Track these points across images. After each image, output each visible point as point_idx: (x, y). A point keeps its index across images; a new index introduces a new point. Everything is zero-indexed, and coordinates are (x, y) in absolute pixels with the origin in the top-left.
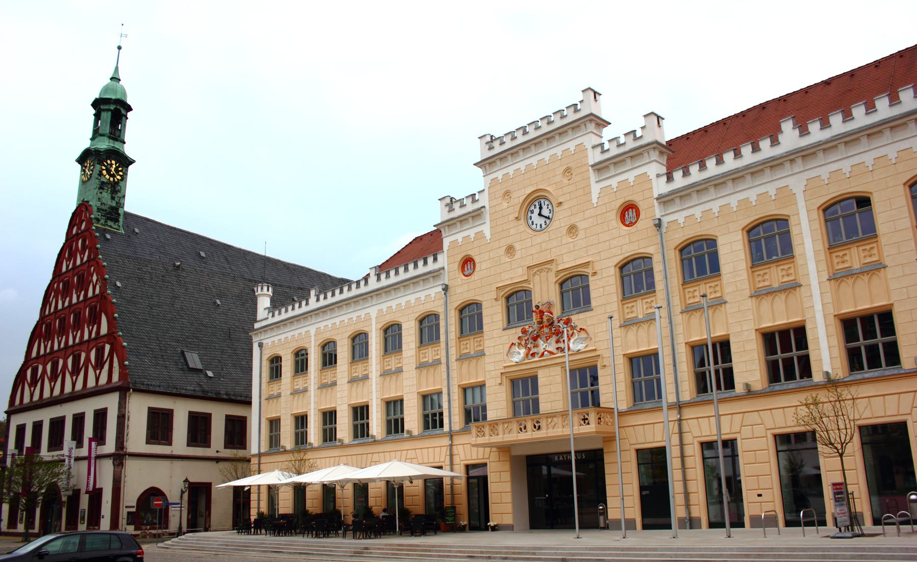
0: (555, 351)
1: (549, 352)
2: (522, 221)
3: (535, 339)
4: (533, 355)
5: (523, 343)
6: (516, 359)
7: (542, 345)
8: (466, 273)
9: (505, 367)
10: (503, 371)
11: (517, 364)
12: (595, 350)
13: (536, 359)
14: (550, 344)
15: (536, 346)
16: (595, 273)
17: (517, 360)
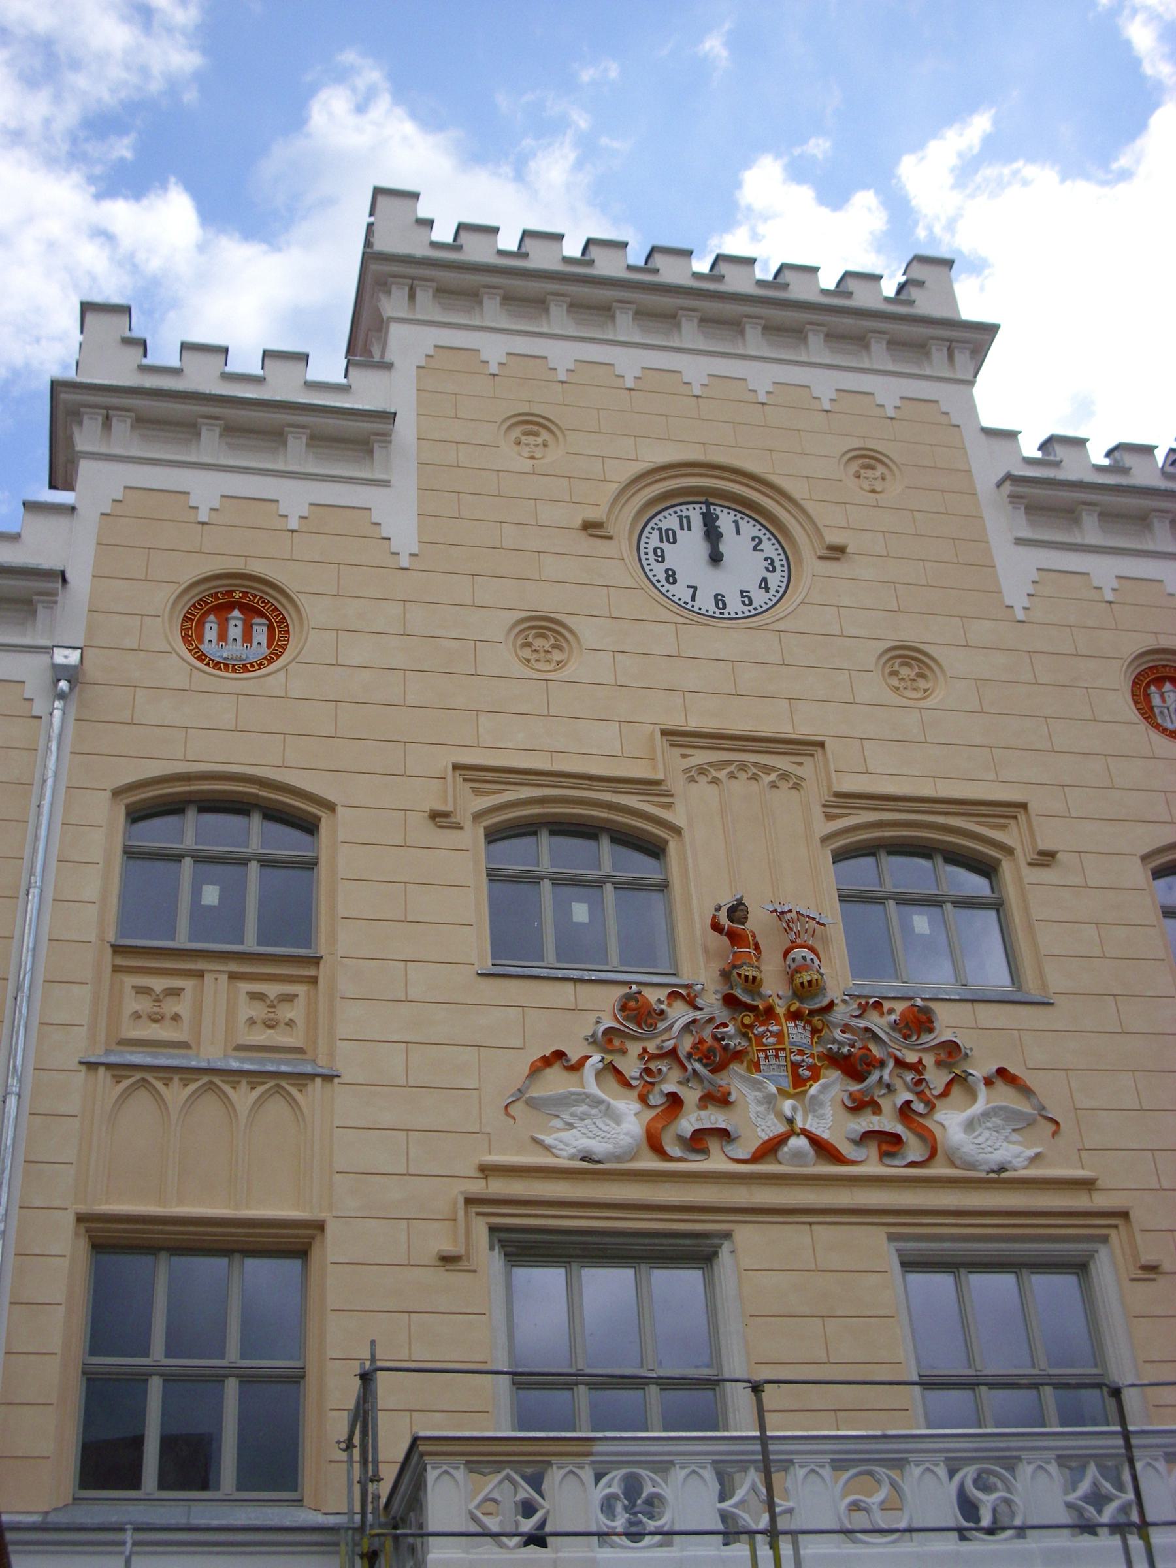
0: (847, 1149)
1: (816, 1142)
2: (623, 545)
3: (717, 1057)
4: (698, 1141)
5: (631, 1067)
6: (570, 1140)
7: (756, 1107)
8: (234, 650)
9: (487, 1171)
10: (478, 1187)
11: (590, 1168)
12: (1087, 1185)
13: (716, 1161)
14: (814, 1106)
15: (722, 1100)
16: (1046, 858)
17: (598, 1147)
